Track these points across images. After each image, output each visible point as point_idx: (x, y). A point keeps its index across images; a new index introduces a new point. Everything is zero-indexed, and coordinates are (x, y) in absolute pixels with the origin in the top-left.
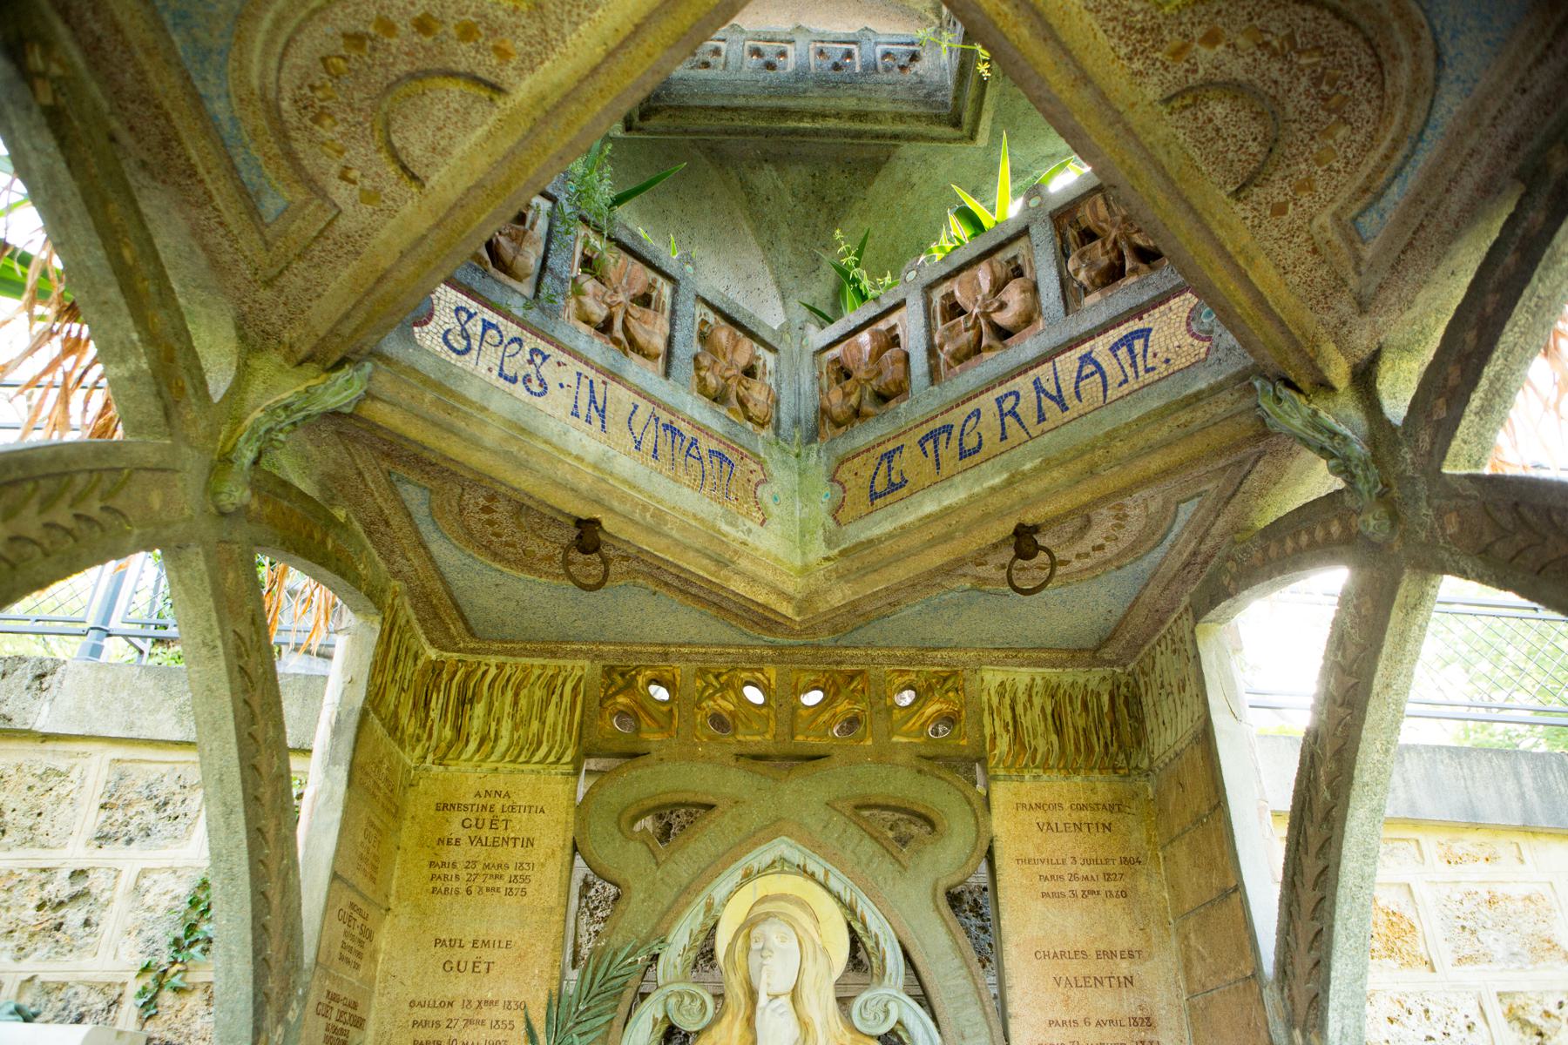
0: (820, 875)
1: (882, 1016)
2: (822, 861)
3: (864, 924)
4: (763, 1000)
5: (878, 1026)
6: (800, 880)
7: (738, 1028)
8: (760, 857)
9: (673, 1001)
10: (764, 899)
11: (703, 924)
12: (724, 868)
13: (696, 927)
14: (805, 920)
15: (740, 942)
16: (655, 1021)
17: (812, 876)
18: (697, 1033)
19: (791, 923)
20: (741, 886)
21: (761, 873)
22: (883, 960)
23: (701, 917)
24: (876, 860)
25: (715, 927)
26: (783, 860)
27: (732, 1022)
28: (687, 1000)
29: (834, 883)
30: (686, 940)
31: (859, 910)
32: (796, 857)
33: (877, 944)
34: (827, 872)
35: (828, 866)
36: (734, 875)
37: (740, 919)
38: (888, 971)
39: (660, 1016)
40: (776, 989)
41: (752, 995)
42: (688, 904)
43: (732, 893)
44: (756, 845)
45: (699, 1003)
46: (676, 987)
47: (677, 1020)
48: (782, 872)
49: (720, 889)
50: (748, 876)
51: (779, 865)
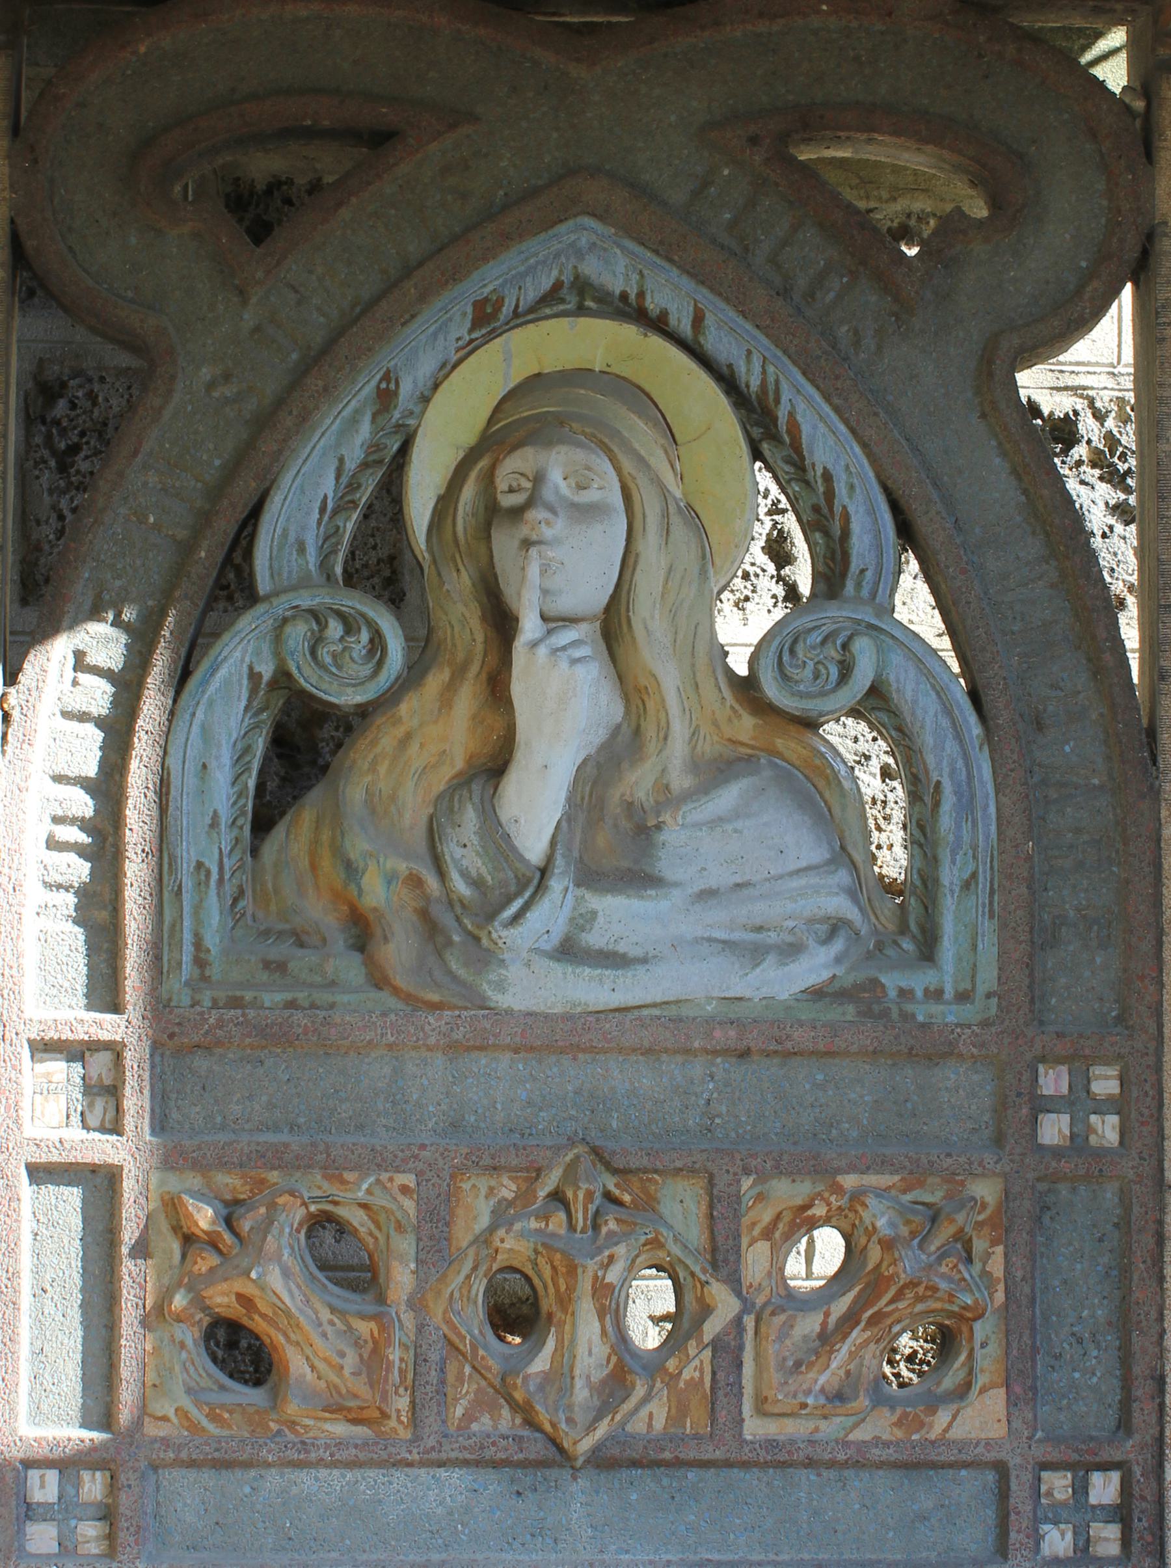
0: (683, 323)
1: (834, 672)
2: (686, 283)
3: (796, 446)
4: (530, 626)
5: (823, 694)
6: (629, 332)
7: (467, 699)
8: (519, 269)
9: (298, 632)
10: (535, 383)
11: (374, 447)
12: (424, 297)
13: (354, 455)
14: (641, 434)
15: (469, 492)
16: (254, 677)
17: (658, 325)
18: (364, 712)
19: (605, 441)
20: (470, 348)
21: (520, 318)
22: (846, 534)
23: (365, 430)
24: (836, 283)
25: (405, 450)
26: (582, 286)
27: (450, 688)
28: (335, 629)
29: (718, 343)
30: (328, 486)
31: (782, 414)
32: (615, 270)
33: (830, 495)
34: (698, 320)
35: (704, 296)
36: (452, 311)
37: (468, 436)
38: (855, 565)
39: (267, 670)
40: (565, 604)
41: (502, 623)
42: (328, 391)
43: (448, 368)
44: (506, 239)
45: (365, 636)
46: (306, 600)
47: (308, 679)
48: (581, 311)
49: (414, 355)
50: (488, 319)
51: (580, 297)
